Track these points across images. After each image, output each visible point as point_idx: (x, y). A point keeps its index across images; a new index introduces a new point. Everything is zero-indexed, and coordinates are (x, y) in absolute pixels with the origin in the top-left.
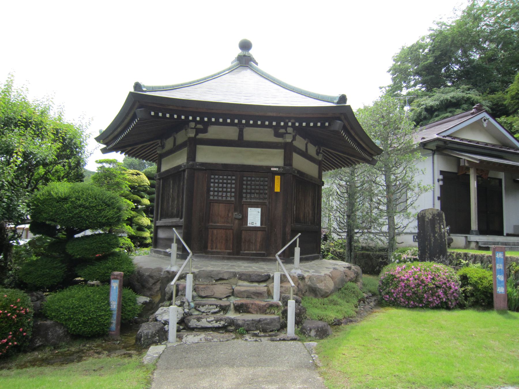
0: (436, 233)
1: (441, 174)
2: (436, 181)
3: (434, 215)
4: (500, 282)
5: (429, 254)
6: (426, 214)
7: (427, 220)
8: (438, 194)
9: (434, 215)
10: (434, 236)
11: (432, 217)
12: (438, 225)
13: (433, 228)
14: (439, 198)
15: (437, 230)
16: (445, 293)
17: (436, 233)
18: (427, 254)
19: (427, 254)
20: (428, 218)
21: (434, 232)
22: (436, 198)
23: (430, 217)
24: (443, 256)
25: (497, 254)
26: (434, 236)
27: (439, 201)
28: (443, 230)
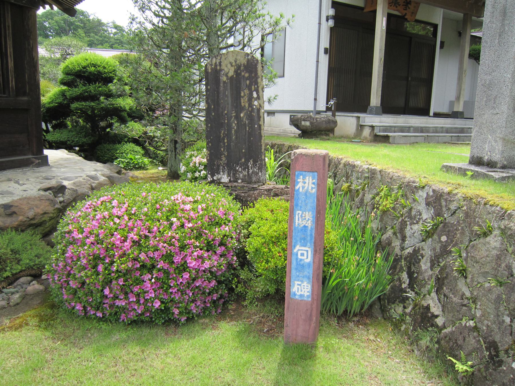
0: (242, 109)
1: (333, 7)
2: (324, 19)
3: (239, 67)
4: (301, 266)
5: (228, 157)
6: (223, 67)
7: (224, 79)
8: (325, 43)
9: (239, 67)
10: (237, 117)
11: (236, 71)
12: (247, 91)
13: (237, 97)
14: (326, 51)
15: (244, 102)
16: (162, 285)
17: (242, 109)
18: (224, 159)
19: (224, 159)
20: (227, 75)
21: (239, 108)
22: (322, 51)
23: (231, 73)
24: (255, 162)
25: (300, 180)
26: (237, 117)
27: (327, 56)
28: (256, 103)
